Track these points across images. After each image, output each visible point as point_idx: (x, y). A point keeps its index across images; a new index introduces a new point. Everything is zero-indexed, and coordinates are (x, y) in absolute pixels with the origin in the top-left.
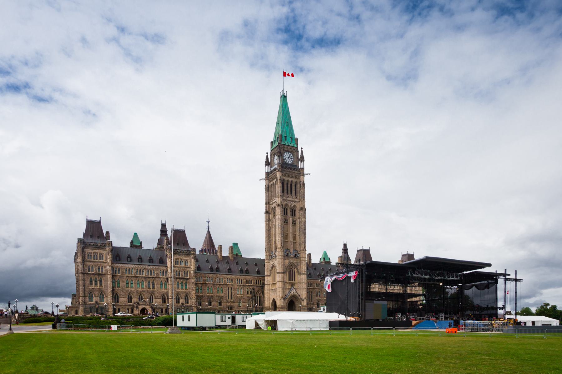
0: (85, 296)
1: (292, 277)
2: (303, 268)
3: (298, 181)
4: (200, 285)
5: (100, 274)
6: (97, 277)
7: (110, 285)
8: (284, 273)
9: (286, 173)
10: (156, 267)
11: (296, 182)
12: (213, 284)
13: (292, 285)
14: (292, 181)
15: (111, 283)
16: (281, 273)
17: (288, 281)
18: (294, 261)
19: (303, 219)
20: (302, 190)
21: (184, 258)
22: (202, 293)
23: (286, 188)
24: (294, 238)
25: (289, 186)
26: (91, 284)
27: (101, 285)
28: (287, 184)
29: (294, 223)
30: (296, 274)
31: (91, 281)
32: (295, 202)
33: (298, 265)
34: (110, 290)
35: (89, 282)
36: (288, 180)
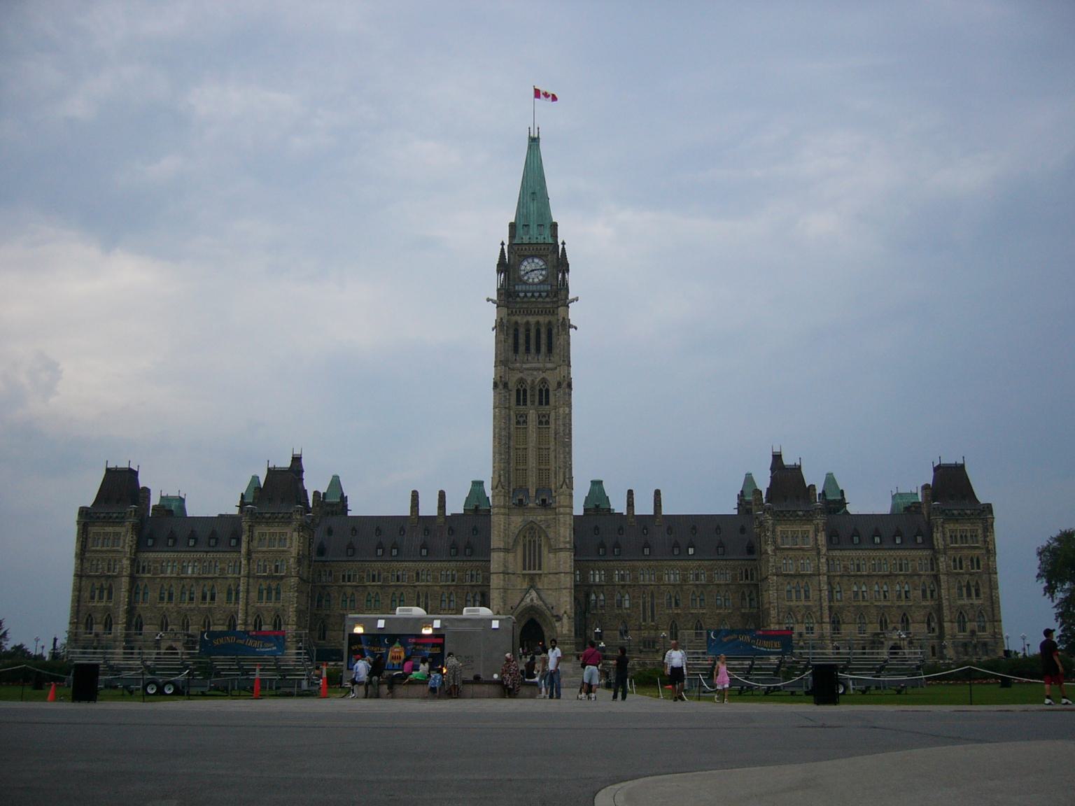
0: (77, 623)
1: (532, 559)
2: (565, 534)
4: (349, 591)
5: (109, 576)
6: (104, 582)
7: (123, 595)
8: (506, 550)
9: (532, 301)
10: (221, 555)
11: (550, 322)
12: (381, 587)
13: (532, 578)
14: (538, 323)
15: (127, 594)
16: (499, 550)
20: (561, 338)
21: (276, 529)
23: (522, 340)
24: (543, 458)
25: (533, 335)
26: (92, 598)
27: (109, 598)
28: (528, 330)
29: (543, 421)
30: (545, 550)
31: (93, 591)
32: (545, 370)
33: (548, 526)
36: (528, 323)
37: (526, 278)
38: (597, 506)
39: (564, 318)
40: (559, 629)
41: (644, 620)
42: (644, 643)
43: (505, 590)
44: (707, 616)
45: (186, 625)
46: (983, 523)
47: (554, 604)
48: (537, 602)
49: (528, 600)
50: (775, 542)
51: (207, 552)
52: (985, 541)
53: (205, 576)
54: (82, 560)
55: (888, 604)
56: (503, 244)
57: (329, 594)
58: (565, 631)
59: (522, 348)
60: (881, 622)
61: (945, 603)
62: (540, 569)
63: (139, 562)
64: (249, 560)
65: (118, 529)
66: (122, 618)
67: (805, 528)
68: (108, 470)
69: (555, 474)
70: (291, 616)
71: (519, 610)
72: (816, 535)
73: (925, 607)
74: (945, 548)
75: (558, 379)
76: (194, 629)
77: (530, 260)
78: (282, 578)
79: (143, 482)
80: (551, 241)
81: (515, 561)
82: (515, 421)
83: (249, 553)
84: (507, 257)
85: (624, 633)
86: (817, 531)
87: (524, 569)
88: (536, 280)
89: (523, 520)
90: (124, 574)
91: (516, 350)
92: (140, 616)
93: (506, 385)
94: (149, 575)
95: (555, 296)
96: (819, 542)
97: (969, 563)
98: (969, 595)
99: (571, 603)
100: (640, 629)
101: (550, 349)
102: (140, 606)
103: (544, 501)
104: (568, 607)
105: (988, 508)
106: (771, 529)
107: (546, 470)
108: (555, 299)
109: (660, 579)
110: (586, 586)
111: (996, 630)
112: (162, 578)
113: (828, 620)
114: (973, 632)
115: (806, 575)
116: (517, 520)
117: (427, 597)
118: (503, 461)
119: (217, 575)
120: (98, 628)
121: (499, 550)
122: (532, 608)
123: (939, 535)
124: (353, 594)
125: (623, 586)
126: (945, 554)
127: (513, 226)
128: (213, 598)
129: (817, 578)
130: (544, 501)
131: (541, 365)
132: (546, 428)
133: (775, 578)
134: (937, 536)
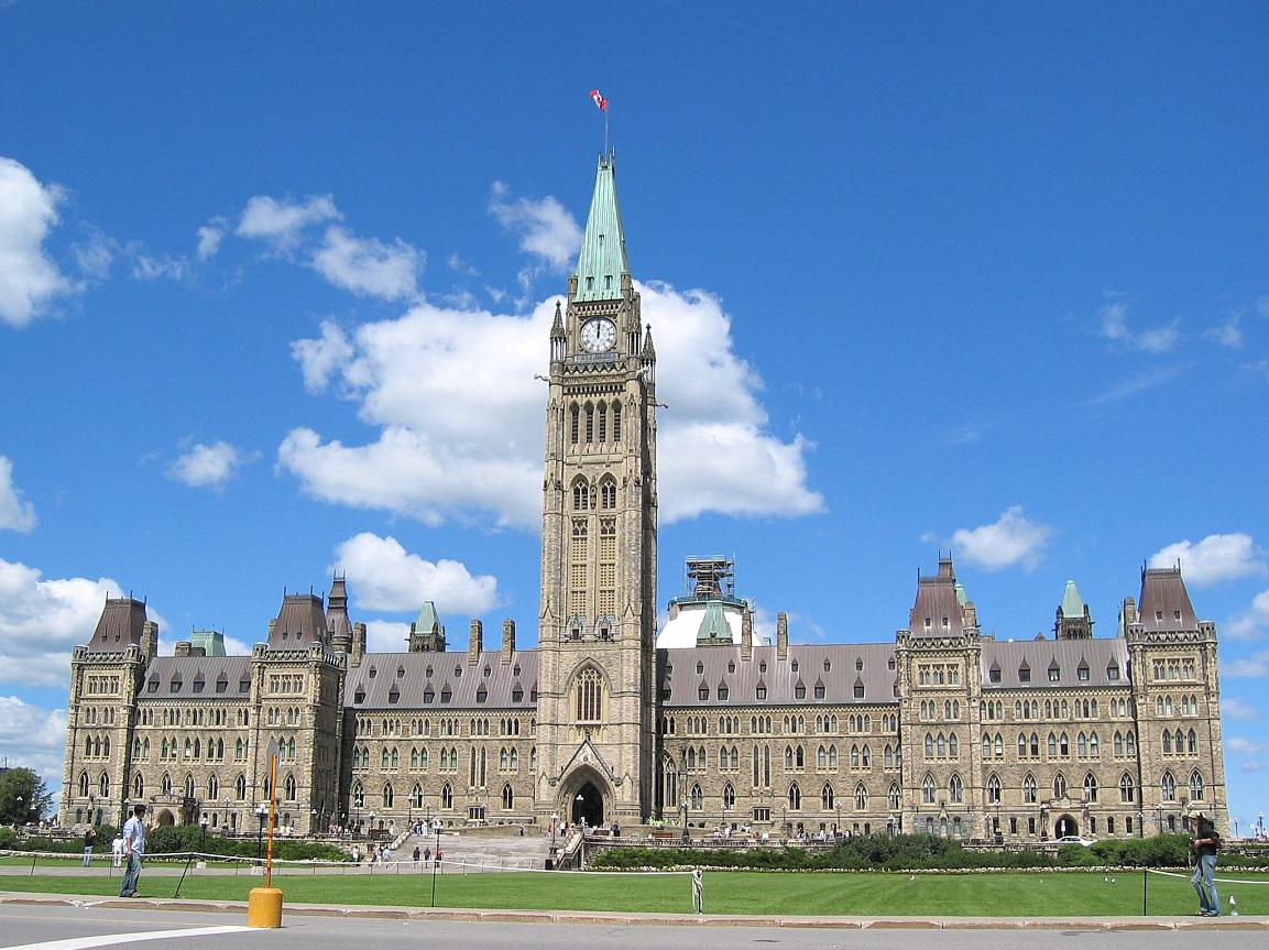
1: (589, 704)
3: (621, 397)
5: (106, 728)
7: (119, 751)
8: (555, 695)
17: (573, 720)
18: (598, 652)
19: (627, 516)
21: (292, 672)
26: (88, 753)
27: (106, 753)
28: (590, 413)
29: (608, 527)
30: (605, 695)
34: (120, 765)
35: (84, 749)
36: (589, 404)
37: (589, 345)
38: (713, 636)
39: (632, 396)
40: (619, 796)
41: (756, 785)
42: (756, 811)
43: (553, 745)
44: (839, 778)
45: (190, 787)
46: (1201, 650)
48: (592, 762)
49: (580, 758)
51: (214, 699)
52: (1204, 675)
53: (212, 727)
54: (77, 708)
55: (1068, 761)
57: (366, 750)
58: (627, 798)
59: (582, 436)
60: (1057, 785)
62: (598, 718)
63: (139, 712)
64: (259, 708)
65: (115, 673)
66: (117, 778)
67: (952, 661)
68: (107, 601)
69: (619, 596)
70: (305, 778)
71: (570, 770)
72: (967, 670)
73: (1118, 766)
75: (625, 474)
76: (199, 792)
77: (595, 323)
78: (296, 730)
79: (152, 615)
80: (619, 297)
81: (567, 709)
82: (572, 529)
83: (259, 699)
84: (564, 321)
85: (729, 800)
86: (968, 664)
87: (579, 718)
88: (602, 348)
90: (122, 725)
91: (575, 440)
92: (140, 775)
93: (559, 486)
94: (151, 727)
95: (623, 366)
98: (1180, 747)
99: (635, 762)
100: (750, 795)
101: (617, 436)
102: (139, 764)
103: (605, 632)
104: (631, 767)
105: (1211, 628)
107: (609, 591)
108: (623, 371)
109: (778, 730)
110: (682, 739)
111: (1217, 798)
112: (164, 730)
113: (980, 784)
114: (1184, 801)
115: (952, 724)
116: (570, 658)
117: (484, 754)
118: (552, 581)
119: (225, 727)
120: (94, 789)
122: (586, 769)
124: (395, 750)
125: (728, 739)
128: (220, 755)
130: (605, 632)
131: (604, 458)
132: (610, 538)
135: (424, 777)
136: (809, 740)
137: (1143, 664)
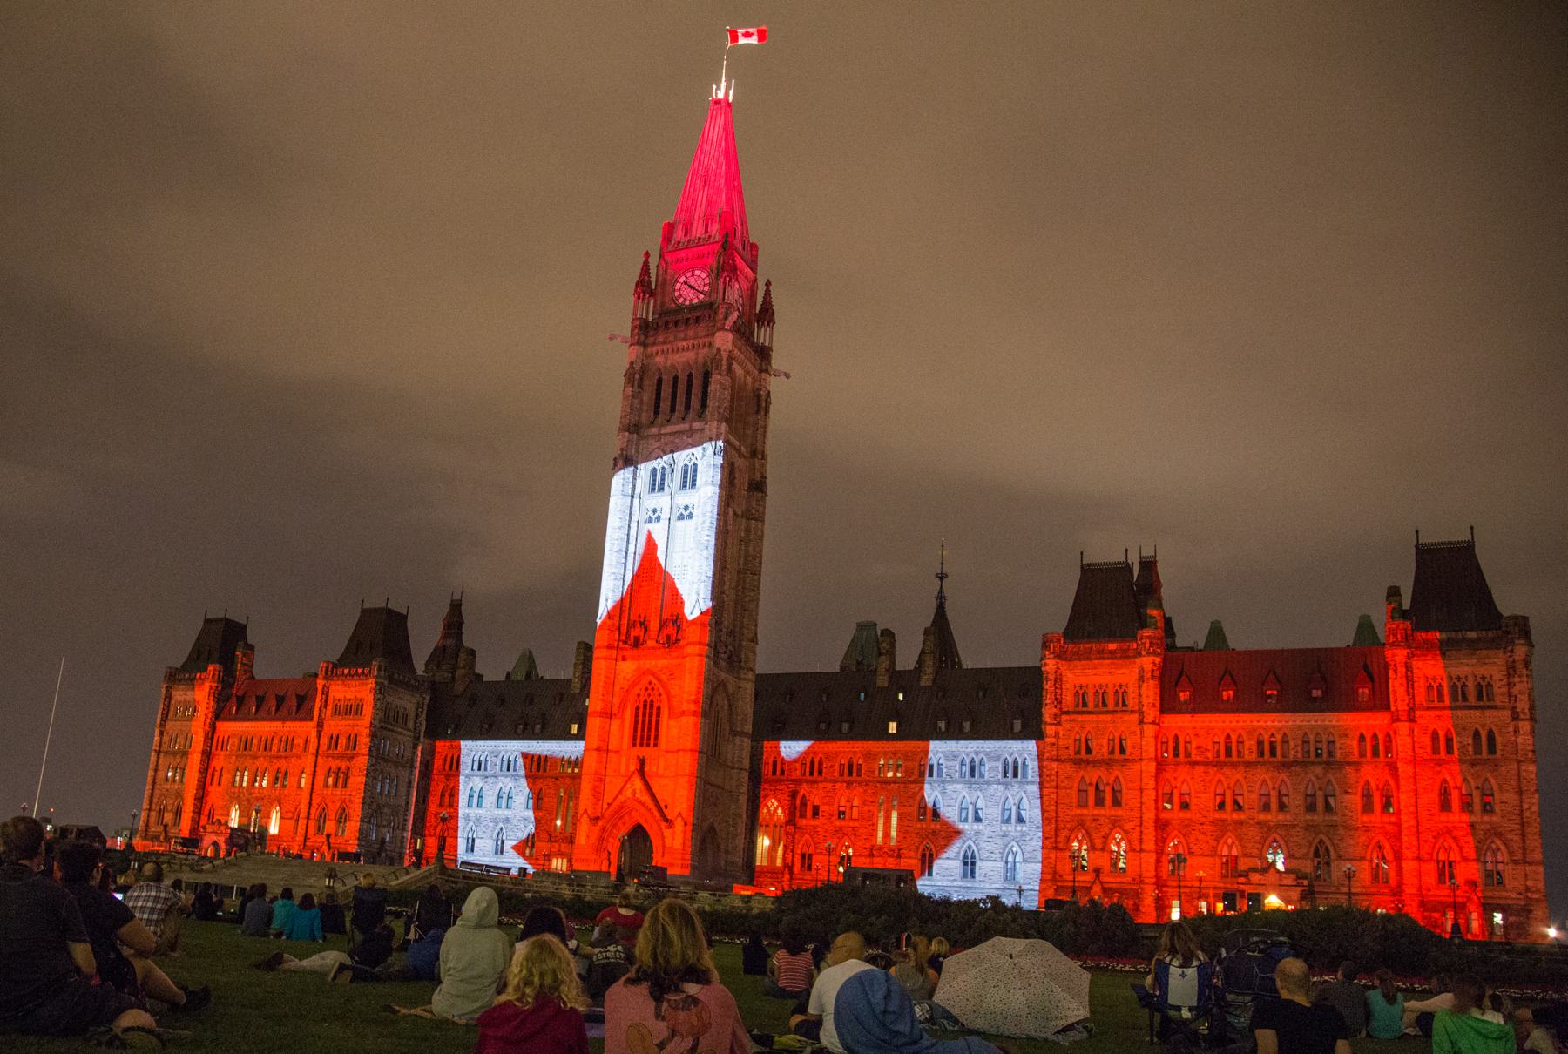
22: (479, 806)
23: (666, 392)
28: (676, 378)
47: (669, 802)
50: (1058, 701)
56: (647, 255)
59: (665, 405)
61: (1407, 822)
74: (1412, 710)
86: (1141, 679)
88: (695, 301)
89: (638, 669)
91: (657, 412)
96: (1145, 702)
97: (1470, 741)
100: (872, 855)
106: (1052, 677)
121: (595, 713)
123: (1397, 683)
126: (1412, 720)
127: (669, 229)
129: (1137, 766)
130: (668, 636)
133: (1054, 765)
134: (1397, 686)
135: (507, 820)
136: (950, 787)
137: (1410, 681)
